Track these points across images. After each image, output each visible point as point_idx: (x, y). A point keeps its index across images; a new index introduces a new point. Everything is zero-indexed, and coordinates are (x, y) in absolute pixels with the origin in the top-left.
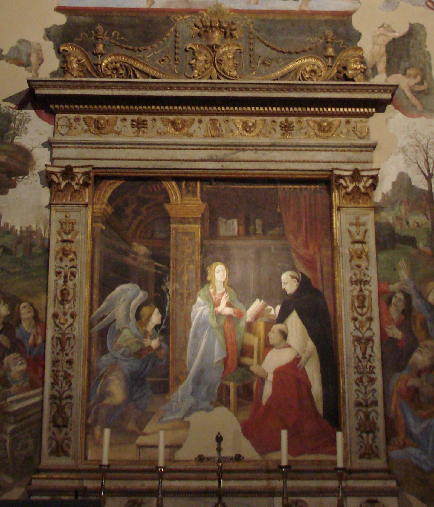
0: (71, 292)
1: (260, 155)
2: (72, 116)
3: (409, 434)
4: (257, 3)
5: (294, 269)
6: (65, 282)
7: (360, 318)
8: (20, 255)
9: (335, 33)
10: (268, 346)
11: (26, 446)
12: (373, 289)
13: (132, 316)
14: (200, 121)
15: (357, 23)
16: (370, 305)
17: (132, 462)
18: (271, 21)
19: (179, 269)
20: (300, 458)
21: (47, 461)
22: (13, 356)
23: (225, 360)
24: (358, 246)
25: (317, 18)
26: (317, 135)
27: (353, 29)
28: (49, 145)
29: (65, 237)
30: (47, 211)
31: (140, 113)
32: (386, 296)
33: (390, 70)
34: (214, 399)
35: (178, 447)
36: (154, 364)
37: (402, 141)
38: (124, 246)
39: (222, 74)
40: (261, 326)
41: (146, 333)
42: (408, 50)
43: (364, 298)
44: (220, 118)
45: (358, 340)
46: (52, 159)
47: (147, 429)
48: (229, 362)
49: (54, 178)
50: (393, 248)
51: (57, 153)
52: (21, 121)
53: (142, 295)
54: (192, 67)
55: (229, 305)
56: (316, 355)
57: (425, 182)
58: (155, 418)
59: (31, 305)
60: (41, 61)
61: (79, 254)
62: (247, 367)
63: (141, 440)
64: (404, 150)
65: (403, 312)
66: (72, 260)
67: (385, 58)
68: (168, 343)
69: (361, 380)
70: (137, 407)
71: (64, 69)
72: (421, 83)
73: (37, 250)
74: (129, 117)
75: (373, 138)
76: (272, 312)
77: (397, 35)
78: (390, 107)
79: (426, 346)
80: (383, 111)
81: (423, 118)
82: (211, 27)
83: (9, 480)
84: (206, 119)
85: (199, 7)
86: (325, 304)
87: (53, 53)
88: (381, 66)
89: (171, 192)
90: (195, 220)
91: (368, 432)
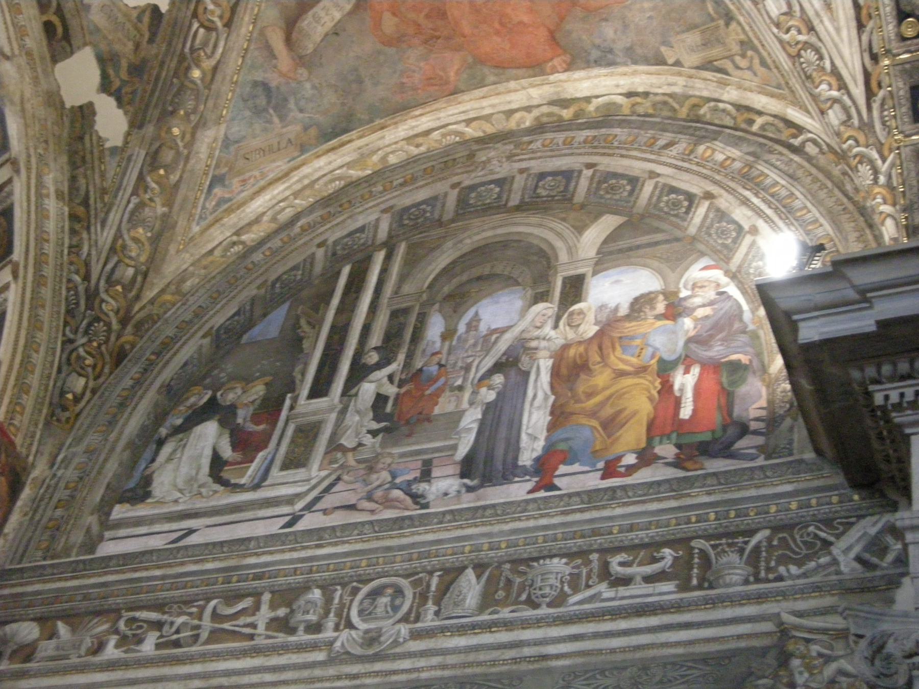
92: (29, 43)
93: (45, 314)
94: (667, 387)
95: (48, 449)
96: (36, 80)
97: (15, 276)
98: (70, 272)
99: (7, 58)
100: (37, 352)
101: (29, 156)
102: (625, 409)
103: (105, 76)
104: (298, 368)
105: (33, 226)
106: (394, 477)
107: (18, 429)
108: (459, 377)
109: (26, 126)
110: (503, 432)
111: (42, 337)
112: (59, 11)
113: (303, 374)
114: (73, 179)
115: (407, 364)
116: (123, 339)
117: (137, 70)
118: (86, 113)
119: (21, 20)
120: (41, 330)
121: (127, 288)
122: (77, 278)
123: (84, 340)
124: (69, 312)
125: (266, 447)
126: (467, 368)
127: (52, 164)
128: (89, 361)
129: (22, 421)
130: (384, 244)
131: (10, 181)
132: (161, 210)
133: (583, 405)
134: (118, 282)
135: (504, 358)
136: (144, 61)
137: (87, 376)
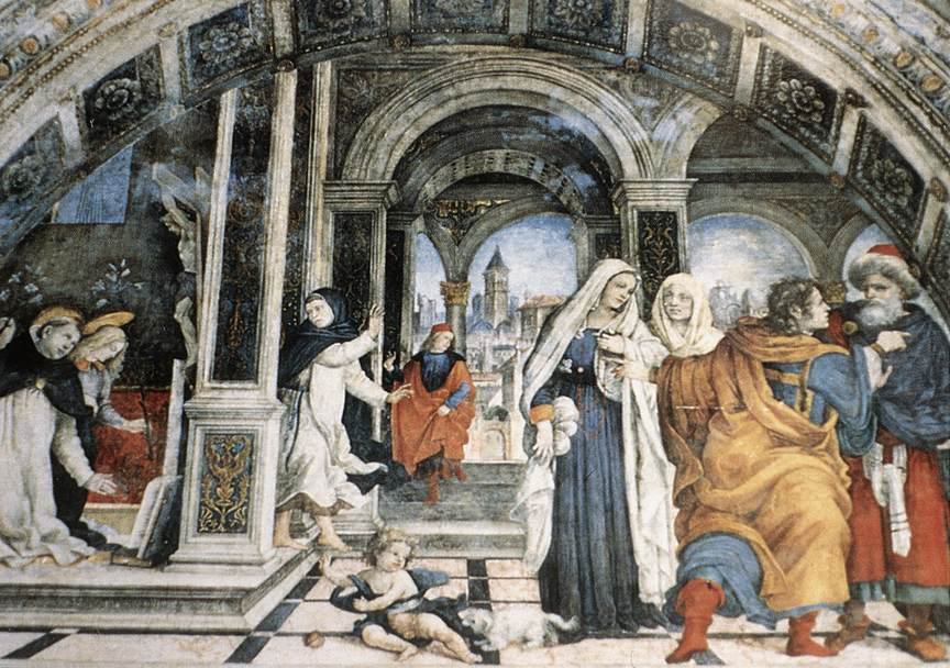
94: (860, 486)
102: (799, 515)
104: (183, 305)
106: (422, 589)
108: (496, 389)
110: (599, 523)
113: (193, 316)
115: (392, 343)
125: (159, 474)
126: (506, 372)
130: (292, 60)
133: (729, 494)
135: (568, 364)
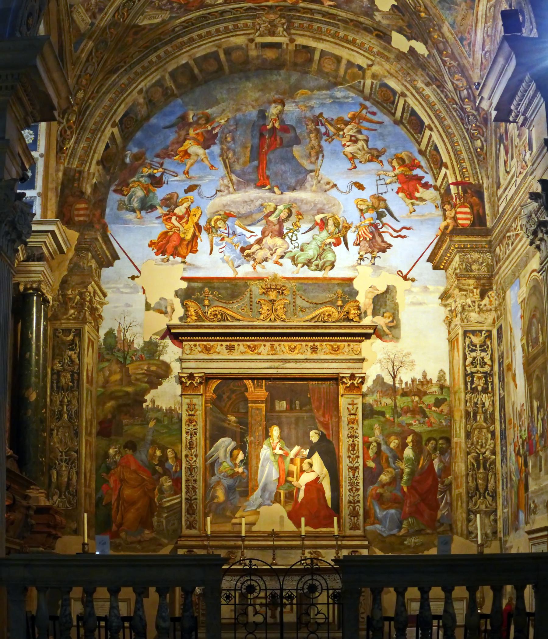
0: (195, 443)
1: (298, 365)
2: (192, 343)
3: (376, 518)
4: (298, 273)
5: (317, 429)
6: (191, 437)
7: (352, 456)
8: (166, 423)
9: (343, 291)
10: (302, 471)
11: (174, 524)
12: (360, 440)
13: (228, 455)
14: (265, 346)
15: (356, 285)
16: (358, 449)
17: (229, 532)
18: (305, 284)
19: (254, 429)
20: (318, 530)
21: (185, 532)
22: (164, 478)
23: (279, 479)
24: (353, 417)
25: (333, 282)
26: (331, 354)
27: (353, 289)
28: (181, 360)
29: (190, 413)
30: (180, 398)
31: (231, 341)
32: (367, 444)
33: (374, 314)
34: (273, 499)
35: (254, 524)
36: (240, 481)
37: (380, 356)
38: (222, 417)
39: (278, 317)
40: (298, 460)
41: (235, 465)
42: (386, 302)
43: (355, 445)
44: (276, 344)
45: (350, 468)
46: (182, 369)
47: (237, 515)
48: (281, 480)
49: (184, 380)
50: (372, 417)
51: (185, 365)
52: (163, 346)
53: (233, 444)
54: (260, 313)
55: (281, 449)
56: (328, 476)
57: (392, 380)
58: (241, 509)
59: (173, 450)
60: (173, 310)
61: (199, 423)
62: (290, 482)
63: (234, 521)
64: (380, 361)
65: (376, 453)
66: (194, 425)
67: (372, 307)
68: (248, 470)
69: (351, 489)
70: (231, 504)
71: (186, 316)
72: (392, 321)
73: (175, 420)
74: (225, 344)
75: (363, 355)
76: (305, 453)
77: (379, 292)
78: (374, 336)
79: (388, 472)
80: (369, 339)
81: (392, 343)
82: (271, 288)
83: (166, 541)
84: (268, 344)
85: (264, 276)
86: (334, 448)
87: (180, 305)
88: (369, 312)
89: (248, 386)
90: (262, 402)
91: (354, 517)
92: (375, 50)
93: (453, 130)
95: (483, 174)
96: (387, 59)
97: (431, 129)
98: (451, 106)
99: (372, 65)
100: (459, 145)
101: (405, 86)
103: (405, 36)
105: (425, 106)
107: (469, 177)
109: (396, 78)
111: (457, 138)
112: (375, 30)
114: (428, 75)
116: (482, 115)
117: (409, 26)
118: (412, 50)
119: (367, 46)
120: (455, 136)
121: (469, 97)
122: (455, 106)
123: (470, 127)
124: (461, 119)
127: (417, 78)
128: (476, 133)
129: (469, 172)
131: (405, 102)
132: (455, 64)
134: (465, 98)
136: (408, 22)
137: (479, 138)
